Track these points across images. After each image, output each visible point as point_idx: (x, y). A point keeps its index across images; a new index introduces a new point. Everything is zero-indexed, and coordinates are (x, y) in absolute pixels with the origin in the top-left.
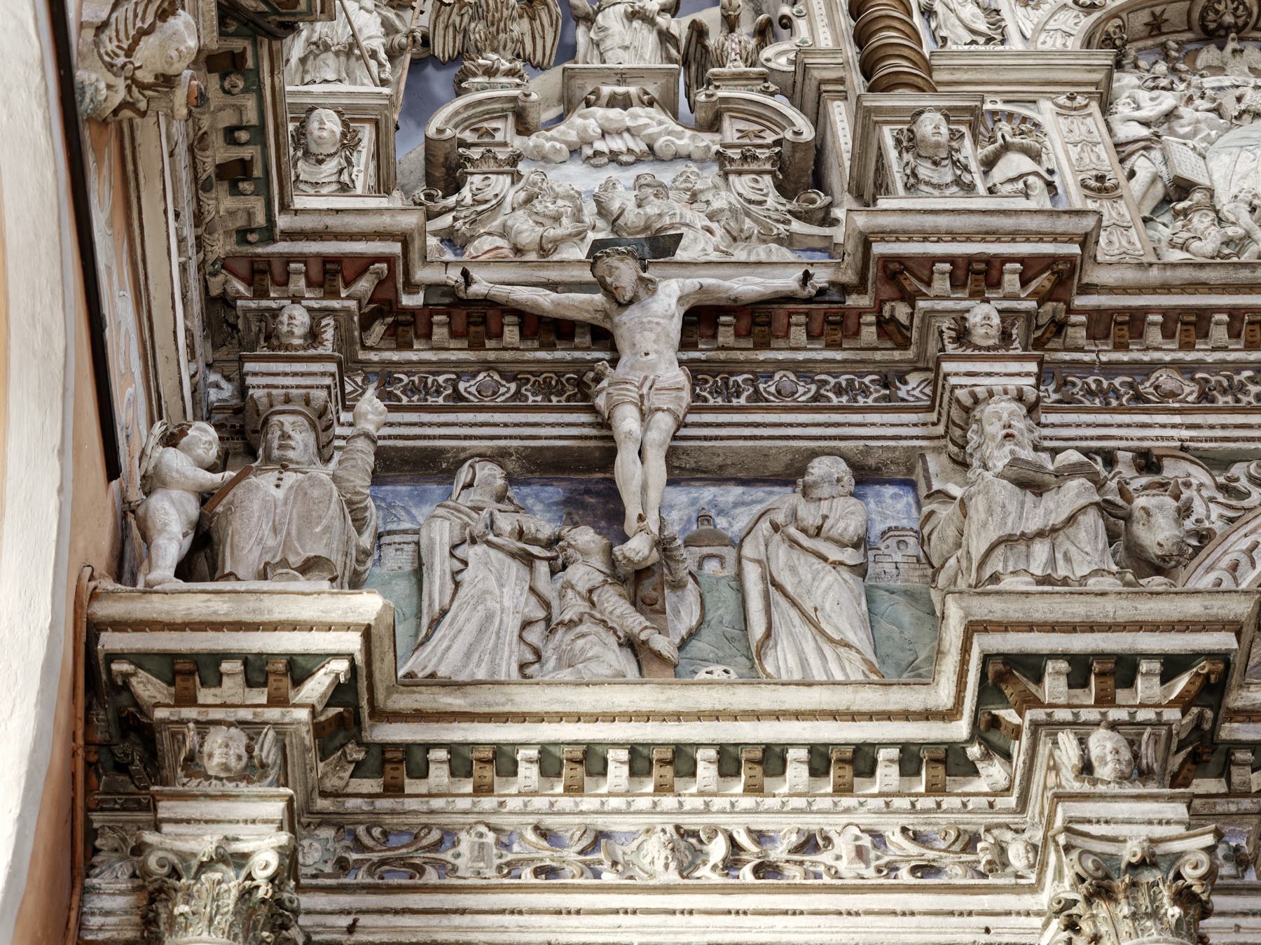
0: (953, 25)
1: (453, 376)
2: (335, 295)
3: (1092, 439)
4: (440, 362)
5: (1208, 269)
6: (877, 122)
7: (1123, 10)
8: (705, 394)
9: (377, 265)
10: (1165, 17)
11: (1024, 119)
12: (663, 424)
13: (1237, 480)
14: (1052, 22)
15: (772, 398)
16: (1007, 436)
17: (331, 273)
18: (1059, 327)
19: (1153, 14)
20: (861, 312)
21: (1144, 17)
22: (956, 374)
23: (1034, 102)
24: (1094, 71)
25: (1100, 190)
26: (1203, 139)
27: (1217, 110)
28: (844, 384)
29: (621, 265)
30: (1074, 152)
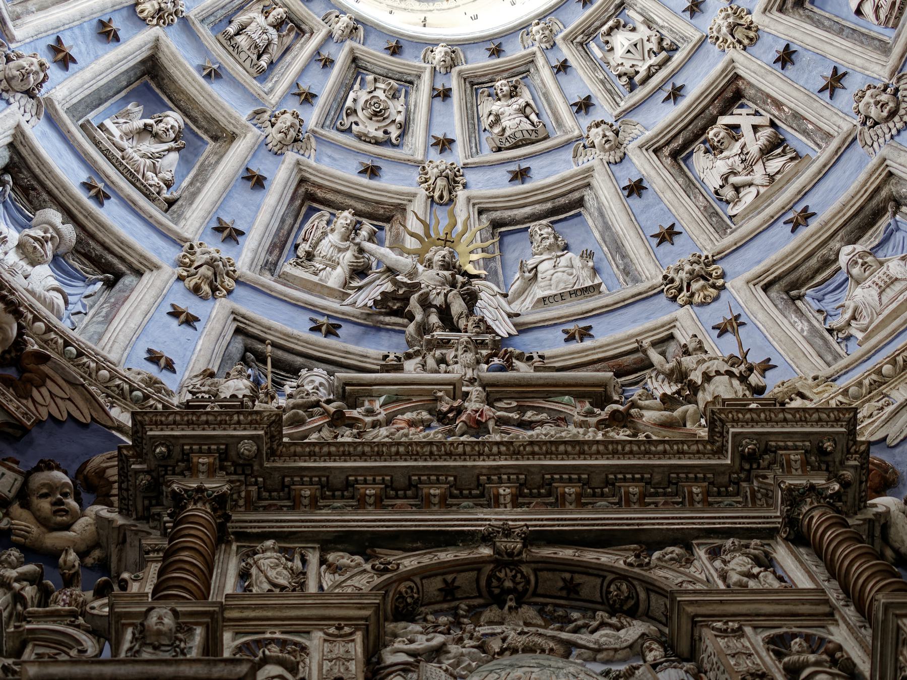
0: (261, 582)
6: (124, 625)
7: (415, 575)
10: (456, 584)
11: (296, 644)
19: (445, 581)
21: (437, 583)
23: (308, 633)
24: (364, 608)
26: (464, 669)
27: (482, 648)
30: (327, 665)
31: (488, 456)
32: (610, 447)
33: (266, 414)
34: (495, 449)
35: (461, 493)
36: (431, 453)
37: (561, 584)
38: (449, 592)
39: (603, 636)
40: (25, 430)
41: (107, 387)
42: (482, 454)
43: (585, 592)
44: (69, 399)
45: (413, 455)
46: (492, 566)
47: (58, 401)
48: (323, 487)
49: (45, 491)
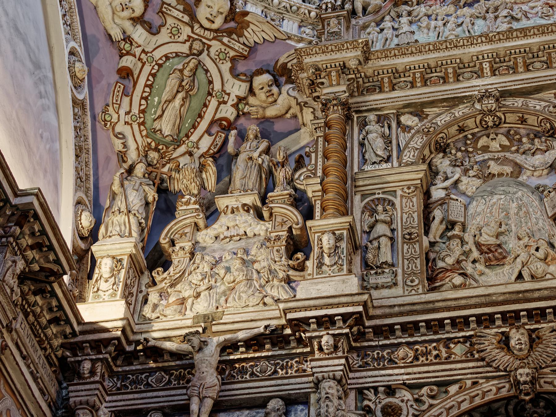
1: (148, 374)
2: (101, 353)
3: (370, 383)
4: (143, 369)
5: (416, 305)
8: (235, 374)
9: (113, 341)
11: (389, 201)
12: (209, 403)
13: (422, 396)
14: (412, 143)
15: (258, 374)
16: (327, 397)
17: (97, 346)
18: (364, 334)
19: (459, 126)
20: (290, 335)
21: (456, 127)
22: (315, 367)
25: (409, 239)
28: (285, 364)
29: (193, 338)
31: (476, 44)
32: (540, 29)
33: (360, 41)
34: (479, 41)
35: (464, 66)
36: (447, 48)
37: (518, 118)
38: (461, 130)
39: (538, 159)
40: (245, 57)
41: (279, 9)
42: (473, 44)
43: (529, 122)
44: (263, 31)
45: (438, 49)
46: (482, 115)
47: (257, 33)
48: (394, 74)
49: (261, 87)
